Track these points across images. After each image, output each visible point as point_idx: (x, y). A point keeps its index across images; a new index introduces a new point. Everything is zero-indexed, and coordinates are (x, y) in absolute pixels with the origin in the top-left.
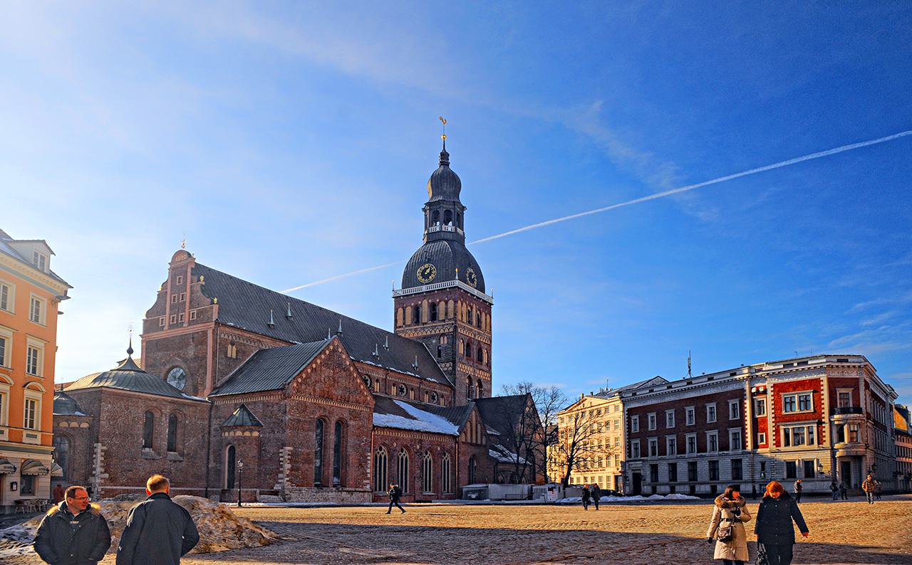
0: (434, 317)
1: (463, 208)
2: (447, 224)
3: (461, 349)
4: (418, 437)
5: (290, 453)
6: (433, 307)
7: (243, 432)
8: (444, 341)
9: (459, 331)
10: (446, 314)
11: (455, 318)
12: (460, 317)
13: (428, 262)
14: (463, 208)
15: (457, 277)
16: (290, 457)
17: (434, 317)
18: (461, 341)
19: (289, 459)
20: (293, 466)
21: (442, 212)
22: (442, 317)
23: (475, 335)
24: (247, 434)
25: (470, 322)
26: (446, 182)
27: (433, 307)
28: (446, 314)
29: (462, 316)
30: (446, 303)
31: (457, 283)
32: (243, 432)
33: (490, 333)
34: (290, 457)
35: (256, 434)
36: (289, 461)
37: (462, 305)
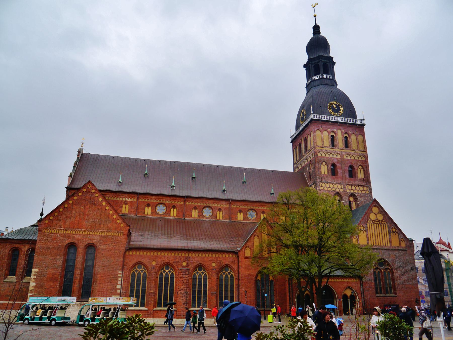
3: (324, 170)
5: (36, 274)
6: (306, 139)
9: (319, 155)
12: (319, 143)
15: (312, 112)
16: (35, 277)
18: (324, 163)
19: (34, 279)
20: (37, 284)
21: (312, 67)
22: (309, 147)
23: (342, 156)
25: (333, 145)
29: (323, 141)
30: (310, 136)
31: (312, 116)
34: (35, 277)
36: (34, 280)
37: (322, 132)
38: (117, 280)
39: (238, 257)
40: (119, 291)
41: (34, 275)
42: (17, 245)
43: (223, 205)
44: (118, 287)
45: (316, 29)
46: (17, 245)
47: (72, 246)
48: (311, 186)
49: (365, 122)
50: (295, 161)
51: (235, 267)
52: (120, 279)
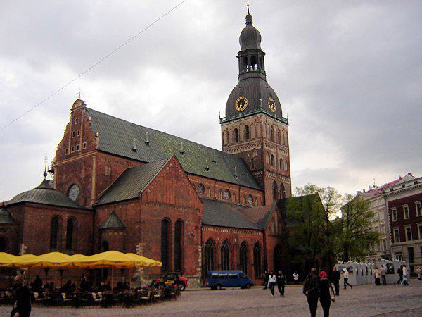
0: (247, 136)
1: (264, 54)
2: (253, 66)
4: (234, 232)
7: (113, 232)
8: (255, 155)
10: (256, 133)
11: (262, 137)
13: (242, 95)
14: (264, 54)
15: (261, 106)
17: (247, 136)
21: (249, 57)
22: (253, 136)
24: (116, 234)
26: (250, 38)
27: (247, 127)
28: (256, 133)
32: (113, 232)
33: (288, 146)
35: (121, 233)
38: (199, 255)
39: (264, 235)
40: (200, 264)
41: (143, 249)
42: (58, 213)
43: (211, 184)
44: (200, 260)
45: (249, 18)
46: (58, 213)
47: (166, 221)
48: (256, 172)
49: (289, 122)
50: (225, 144)
51: (262, 243)
52: (200, 253)
